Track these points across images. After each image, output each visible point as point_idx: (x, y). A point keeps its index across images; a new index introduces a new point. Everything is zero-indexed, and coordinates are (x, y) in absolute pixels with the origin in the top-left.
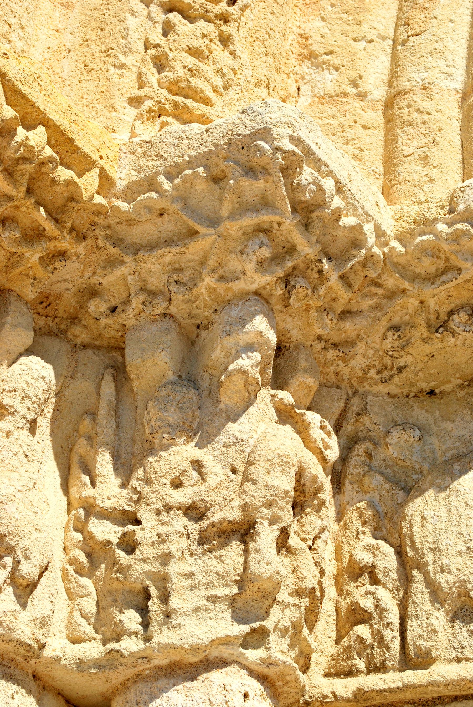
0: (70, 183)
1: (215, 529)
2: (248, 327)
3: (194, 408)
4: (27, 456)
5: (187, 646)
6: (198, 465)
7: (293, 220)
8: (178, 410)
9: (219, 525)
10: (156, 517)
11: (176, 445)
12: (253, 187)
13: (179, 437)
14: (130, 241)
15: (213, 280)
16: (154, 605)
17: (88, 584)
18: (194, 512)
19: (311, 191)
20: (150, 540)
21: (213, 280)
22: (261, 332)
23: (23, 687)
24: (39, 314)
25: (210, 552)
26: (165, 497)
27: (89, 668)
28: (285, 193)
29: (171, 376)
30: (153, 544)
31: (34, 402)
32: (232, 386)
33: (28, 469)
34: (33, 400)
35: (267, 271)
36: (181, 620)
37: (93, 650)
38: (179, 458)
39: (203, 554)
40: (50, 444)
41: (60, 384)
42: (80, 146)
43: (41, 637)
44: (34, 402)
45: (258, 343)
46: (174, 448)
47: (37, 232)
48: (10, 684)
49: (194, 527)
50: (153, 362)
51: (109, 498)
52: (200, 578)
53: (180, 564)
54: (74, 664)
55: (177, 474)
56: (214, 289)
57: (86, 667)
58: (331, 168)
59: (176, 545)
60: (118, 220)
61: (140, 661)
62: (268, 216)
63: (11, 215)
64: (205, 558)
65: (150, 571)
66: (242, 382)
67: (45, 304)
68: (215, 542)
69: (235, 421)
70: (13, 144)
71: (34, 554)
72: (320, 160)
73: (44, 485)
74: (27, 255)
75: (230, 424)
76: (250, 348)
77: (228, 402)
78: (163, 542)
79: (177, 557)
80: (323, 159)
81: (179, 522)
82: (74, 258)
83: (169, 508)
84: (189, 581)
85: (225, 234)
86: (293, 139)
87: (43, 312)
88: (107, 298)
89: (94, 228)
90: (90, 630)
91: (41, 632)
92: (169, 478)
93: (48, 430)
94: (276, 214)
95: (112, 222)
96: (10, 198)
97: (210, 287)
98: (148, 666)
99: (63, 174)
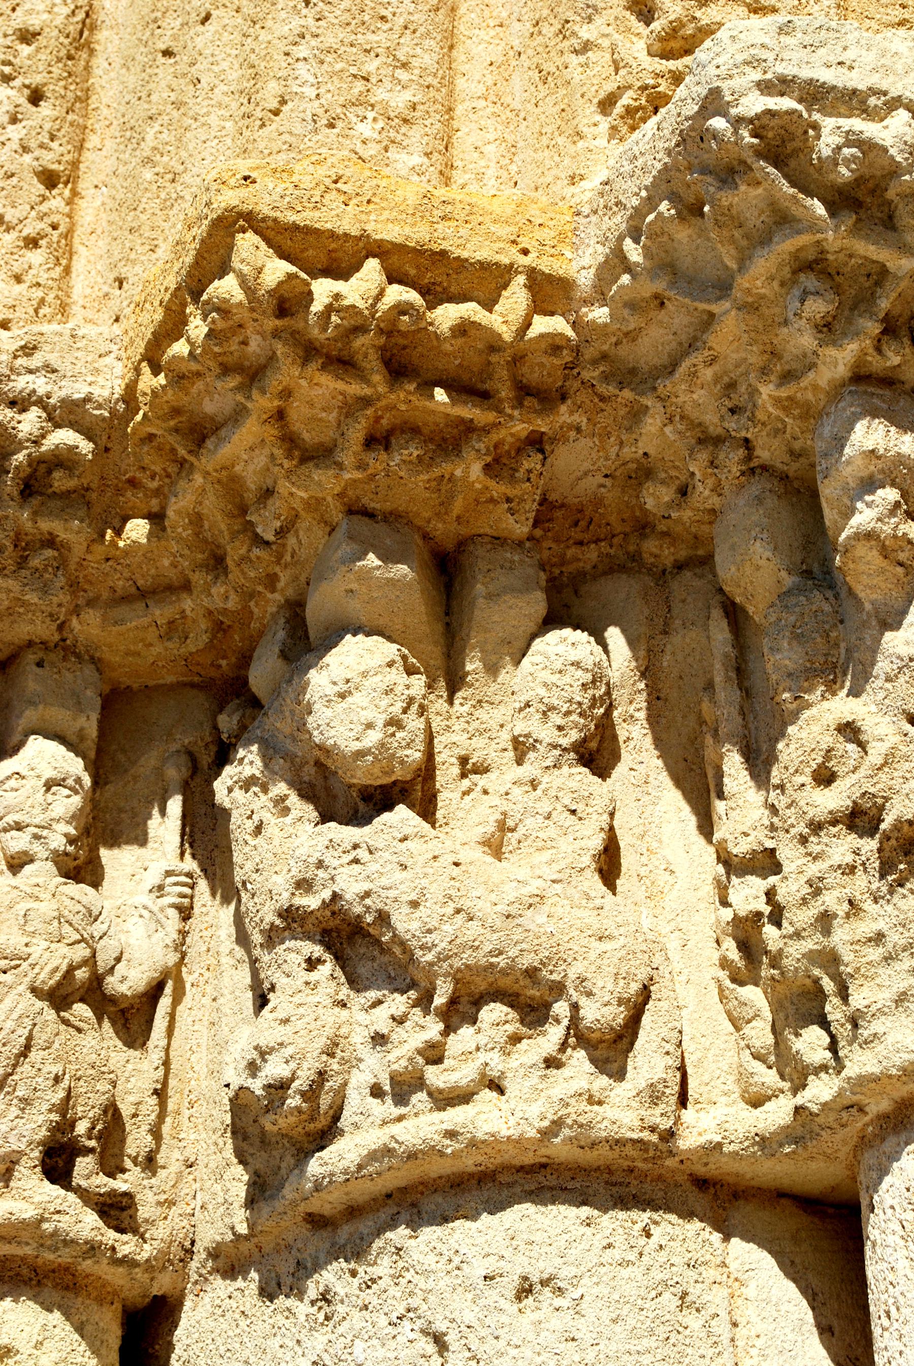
0: (463, 329)
1: (893, 842)
2: (847, 450)
3: (827, 627)
4: (573, 812)
5: (894, 1071)
6: (850, 731)
7: (837, 227)
8: (795, 643)
9: (896, 834)
10: (802, 850)
11: (809, 706)
12: (745, 199)
13: (809, 691)
14: (646, 368)
15: (771, 386)
16: (834, 1010)
17: (752, 997)
18: (860, 818)
19: (847, 162)
20: (799, 895)
21: (771, 386)
22: (873, 451)
23: (669, 1210)
24: (581, 543)
25: (901, 885)
26: (805, 809)
27: (781, 1145)
28: (792, 191)
29: (789, 580)
30: (804, 901)
31: (568, 713)
32: (862, 567)
33: (578, 834)
34: (564, 709)
35: (844, 334)
36: (877, 1026)
37: (777, 1114)
38: (816, 728)
39: (891, 892)
40: (660, 763)
41: (642, 653)
42: (465, 254)
43: (658, 1120)
44: (568, 713)
45: (882, 471)
46: (806, 714)
47: (462, 428)
48: (635, 1214)
49: (870, 845)
50: (754, 567)
51: (746, 834)
52: (895, 938)
53: (854, 923)
54: (753, 1145)
55: (820, 760)
56: (790, 398)
57: (775, 1146)
58: (894, 93)
59: (836, 893)
60: (614, 339)
61: (844, 1114)
62: (788, 242)
63: (398, 421)
64: (896, 899)
65: (811, 951)
66: (875, 552)
67: (583, 524)
68: (902, 866)
69: (896, 625)
70: (312, 319)
71: (600, 984)
72: (854, 91)
73: (660, 841)
74: (458, 473)
75: (888, 636)
76: (869, 485)
77: (875, 596)
78: (817, 892)
79: (841, 913)
80: (862, 87)
81: (843, 846)
82: (573, 434)
83: (816, 827)
84: (881, 950)
85: (750, 300)
86: (765, 87)
87: (587, 537)
88: (663, 475)
89: (575, 371)
90: (770, 1077)
91: (658, 1111)
92: (808, 771)
93: (649, 739)
94: (799, 232)
95: (605, 347)
96: (366, 402)
97: (777, 401)
98: (867, 1119)
99: (447, 315)
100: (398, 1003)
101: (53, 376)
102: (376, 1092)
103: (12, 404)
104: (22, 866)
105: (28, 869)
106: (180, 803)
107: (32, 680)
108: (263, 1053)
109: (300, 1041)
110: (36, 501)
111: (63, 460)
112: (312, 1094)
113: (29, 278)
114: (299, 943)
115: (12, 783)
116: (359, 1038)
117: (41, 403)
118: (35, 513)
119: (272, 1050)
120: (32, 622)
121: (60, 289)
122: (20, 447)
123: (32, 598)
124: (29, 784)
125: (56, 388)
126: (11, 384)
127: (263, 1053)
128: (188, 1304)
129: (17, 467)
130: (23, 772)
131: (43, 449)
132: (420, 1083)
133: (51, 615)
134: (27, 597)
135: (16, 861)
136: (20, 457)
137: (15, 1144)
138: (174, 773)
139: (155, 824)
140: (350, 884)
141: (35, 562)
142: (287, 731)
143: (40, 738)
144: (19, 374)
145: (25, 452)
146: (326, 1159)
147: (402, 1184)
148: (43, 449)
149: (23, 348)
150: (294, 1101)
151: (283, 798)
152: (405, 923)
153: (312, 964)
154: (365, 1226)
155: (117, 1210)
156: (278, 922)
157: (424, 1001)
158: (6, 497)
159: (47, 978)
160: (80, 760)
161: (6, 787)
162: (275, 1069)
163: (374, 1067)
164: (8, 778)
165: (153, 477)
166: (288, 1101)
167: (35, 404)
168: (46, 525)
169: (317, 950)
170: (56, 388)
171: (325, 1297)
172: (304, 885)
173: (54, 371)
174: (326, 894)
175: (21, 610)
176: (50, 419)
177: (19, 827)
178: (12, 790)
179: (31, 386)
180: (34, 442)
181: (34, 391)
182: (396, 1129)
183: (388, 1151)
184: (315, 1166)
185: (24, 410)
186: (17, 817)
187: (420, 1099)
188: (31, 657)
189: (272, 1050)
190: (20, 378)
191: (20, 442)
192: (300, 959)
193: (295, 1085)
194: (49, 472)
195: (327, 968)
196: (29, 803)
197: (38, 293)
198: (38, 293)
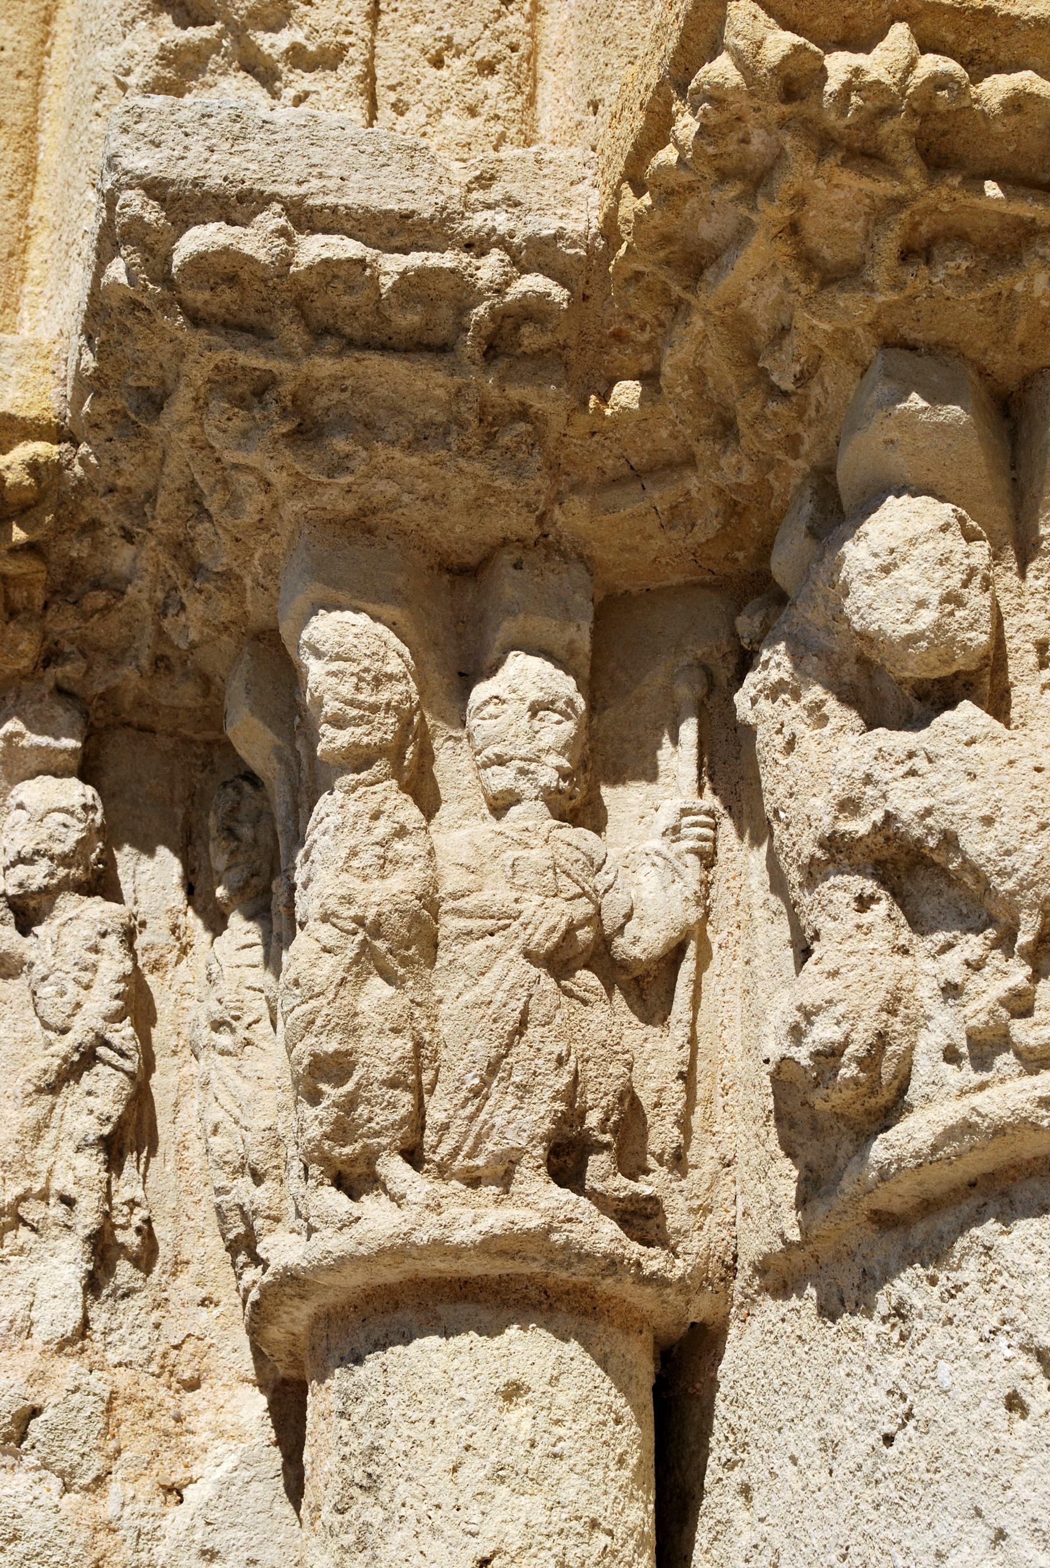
0: (1018, 103)
42: (1016, 11)
47: (1020, 231)
63: (940, 228)
70: (827, 102)
74: (1019, 287)
96: (898, 203)
99: (995, 89)
100: (973, 945)
101: (516, 211)
102: (951, 1055)
103: (468, 247)
104: (506, 808)
105: (514, 811)
106: (695, 728)
107: (508, 584)
108: (809, 1014)
110: (502, 364)
111: (533, 311)
112: (870, 1061)
113: (485, 110)
114: (846, 878)
115: (491, 709)
116: (926, 991)
117: (503, 243)
118: (502, 379)
119: (818, 1010)
120: (505, 515)
121: (523, 122)
122: (480, 297)
123: (504, 483)
124: (510, 709)
125: (520, 225)
126: (466, 223)
127: (809, 1014)
128: (733, 1332)
129: (477, 323)
130: (505, 696)
131: (508, 298)
132: (1004, 1042)
133: (528, 505)
134: (497, 484)
135: (500, 802)
137: (514, 1140)
138: (685, 692)
139: (665, 754)
140: (906, 801)
141: (506, 439)
142: (820, 622)
143: (522, 654)
144: (475, 211)
145: (486, 304)
146: (892, 1140)
147: (988, 1168)
148: (508, 298)
149: (477, 179)
150: (848, 1071)
151: (819, 705)
152: (978, 845)
153: (864, 903)
154: (945, 1222)
155: (640, 1218)
156: (819, 854)
157: (1005, 942)
158: (466, 361)
159: (542, 940)
160: (571, 679)
161: (484, 714)
162: (824, 1032)
163: (946, 1025)
164: (486, 703)
165: (642, 329)
166: (842, 1071)
167: (495, 245)
168: (516, 393)
169: (870, 886)
170: (520, 225)
171: (900, 1312)
172: (849, 806)
173: (517, 204)
174: (878, 816)
175: (492, 500)
176: (514, 262)
177: (501, 761)
178: (491, 717)
179: (490, 224)
180: (497, 291)
181: (494, 229)
182: (978, 1100)
183: (967, 1127)
184: (878, 1151)
185: (483, 254)
186: (497, 749)
187: (1005, 1060)
188: (507, 558)
189: (818, 1010)
190: (477, 215)
191: (480, 292)
192: (848, 897)
193: (850, 1050)
194: (517, 328)
195: (881, 908)
196: (512, 731)
197: (498, 128)
198: (498, 128)
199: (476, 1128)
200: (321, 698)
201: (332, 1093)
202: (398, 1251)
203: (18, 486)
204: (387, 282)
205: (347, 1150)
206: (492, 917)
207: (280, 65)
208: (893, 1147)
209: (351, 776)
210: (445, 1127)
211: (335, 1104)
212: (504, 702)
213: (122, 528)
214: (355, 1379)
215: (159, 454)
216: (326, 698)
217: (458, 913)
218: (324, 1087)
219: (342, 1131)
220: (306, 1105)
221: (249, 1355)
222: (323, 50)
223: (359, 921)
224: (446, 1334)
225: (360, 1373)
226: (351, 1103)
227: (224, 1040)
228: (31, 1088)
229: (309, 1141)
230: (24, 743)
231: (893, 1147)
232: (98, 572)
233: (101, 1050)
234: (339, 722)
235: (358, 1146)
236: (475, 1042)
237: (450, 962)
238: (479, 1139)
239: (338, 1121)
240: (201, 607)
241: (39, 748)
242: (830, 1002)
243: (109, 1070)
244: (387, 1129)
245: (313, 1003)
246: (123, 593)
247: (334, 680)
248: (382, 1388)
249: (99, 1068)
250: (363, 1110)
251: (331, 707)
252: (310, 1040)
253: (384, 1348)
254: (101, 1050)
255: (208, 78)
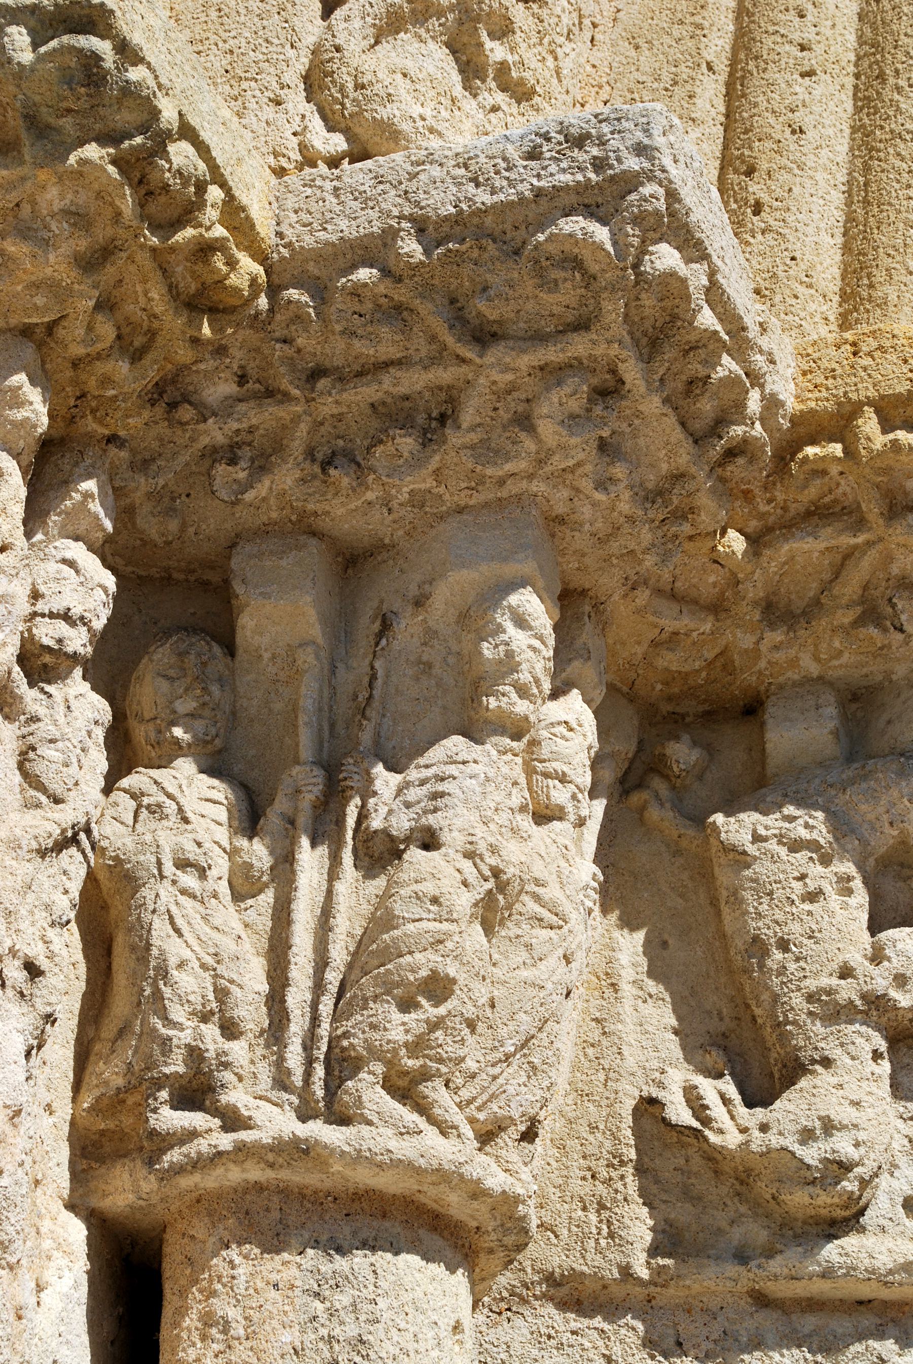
105: (556, 824)
106: (603, 807)
108: (829, 1126)
109: (871, 1129)
112: (864, 1183)
119: (843, 1127)
127: (829, 1126)
135: (549, 812)
136: (738, 430)
137: (516, 1114)
142: (871, 816)
146: (849, 1249)
147: (887, 1298)
150: (850, 1185)
151: (849, 879)
153: (877, 1055)
154: (841, 1324)
156: (858, 1002)
162: (842, 1146)
164: (559, 723)
165: (769, 501)
166: (844, 1183)
169: (883, 1046)
184: (831, 1252)
186: (565, 768)
189: (843, 1127)
192: (868, 1048)
193: (858, 1170)
195: (885, 1067)
199: (493, 1088)
200: (519, 664)
201: (429, 1010)
202: (443, 1176)
203: (237, 290)
204: (721, 372)
205: (410, 1063)
206: (557, 915)
207: (490, 71)
208: (847, 1255)
209: (508, 741)
210: (473, 1076)
211: (427, 1021)
212: (571, 730)
213: (241, 367)
214: (337, 1266)
215: (394, 352)
216: (524, 666)
217: (537, 898)
218: (423, 1001)
219: (417, 1047)
220: (393, 1008)
221: (67, 1175)
222: (521, 82)
223: (496, 873)
224: (427, 1258)
225: (341, 1263)
226: (435, 1025)
227: (189, 880)
228: (35, 845)
229: (389, 1042)
230: (91, 506)
231: (847, 1255)
232: (191, 388)
233: (82, 836)
234: (523, 692)
235: (421, 1062)
236: (522, 1016)
237: (518, 937)
238: (493, 1097)
239: (420, 1037)
240: (289, 482)
241: (97, 518)
242: (855, 1126)
243: (80, 857)
244: (450, 1060)
245: (445, 926)
246: (205, 420)
247: (531, 654)
248: (371, 1288)
249: (73, 850)
250: (439, 1034)
251: (524, 677)
252: (430, 955)
253: (373, 1249)
254: (82, 836)
255: (422, 31)
